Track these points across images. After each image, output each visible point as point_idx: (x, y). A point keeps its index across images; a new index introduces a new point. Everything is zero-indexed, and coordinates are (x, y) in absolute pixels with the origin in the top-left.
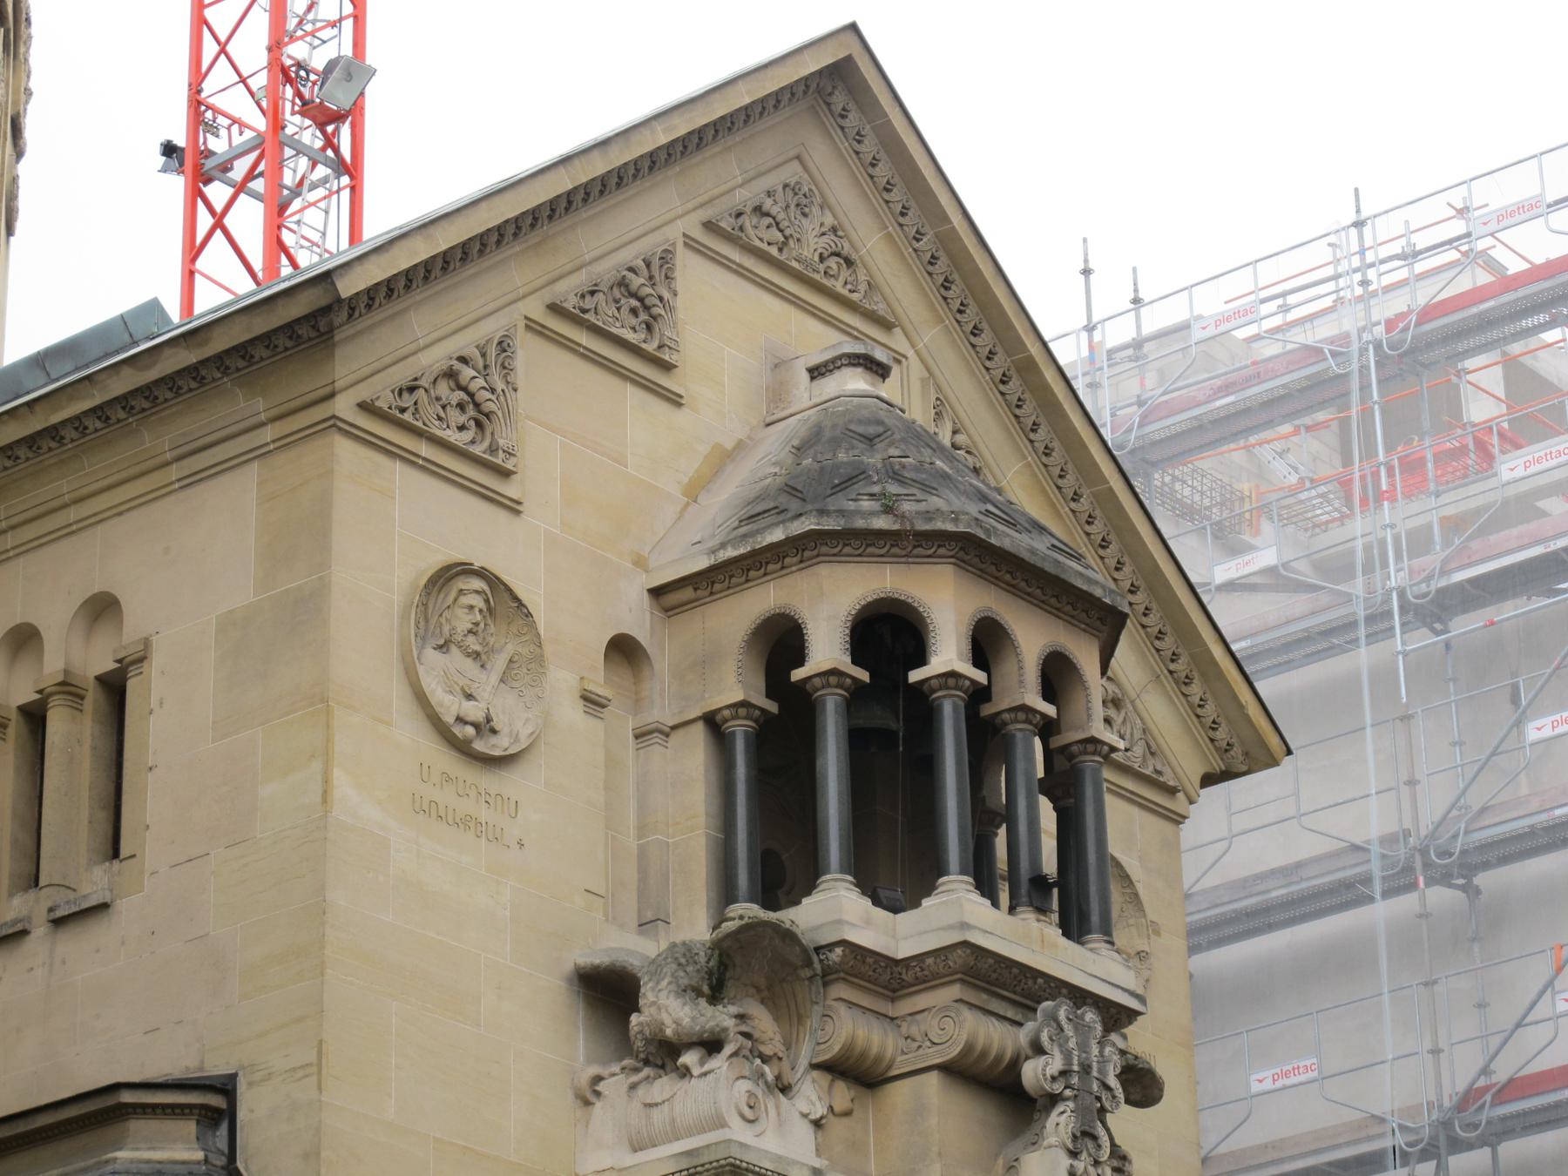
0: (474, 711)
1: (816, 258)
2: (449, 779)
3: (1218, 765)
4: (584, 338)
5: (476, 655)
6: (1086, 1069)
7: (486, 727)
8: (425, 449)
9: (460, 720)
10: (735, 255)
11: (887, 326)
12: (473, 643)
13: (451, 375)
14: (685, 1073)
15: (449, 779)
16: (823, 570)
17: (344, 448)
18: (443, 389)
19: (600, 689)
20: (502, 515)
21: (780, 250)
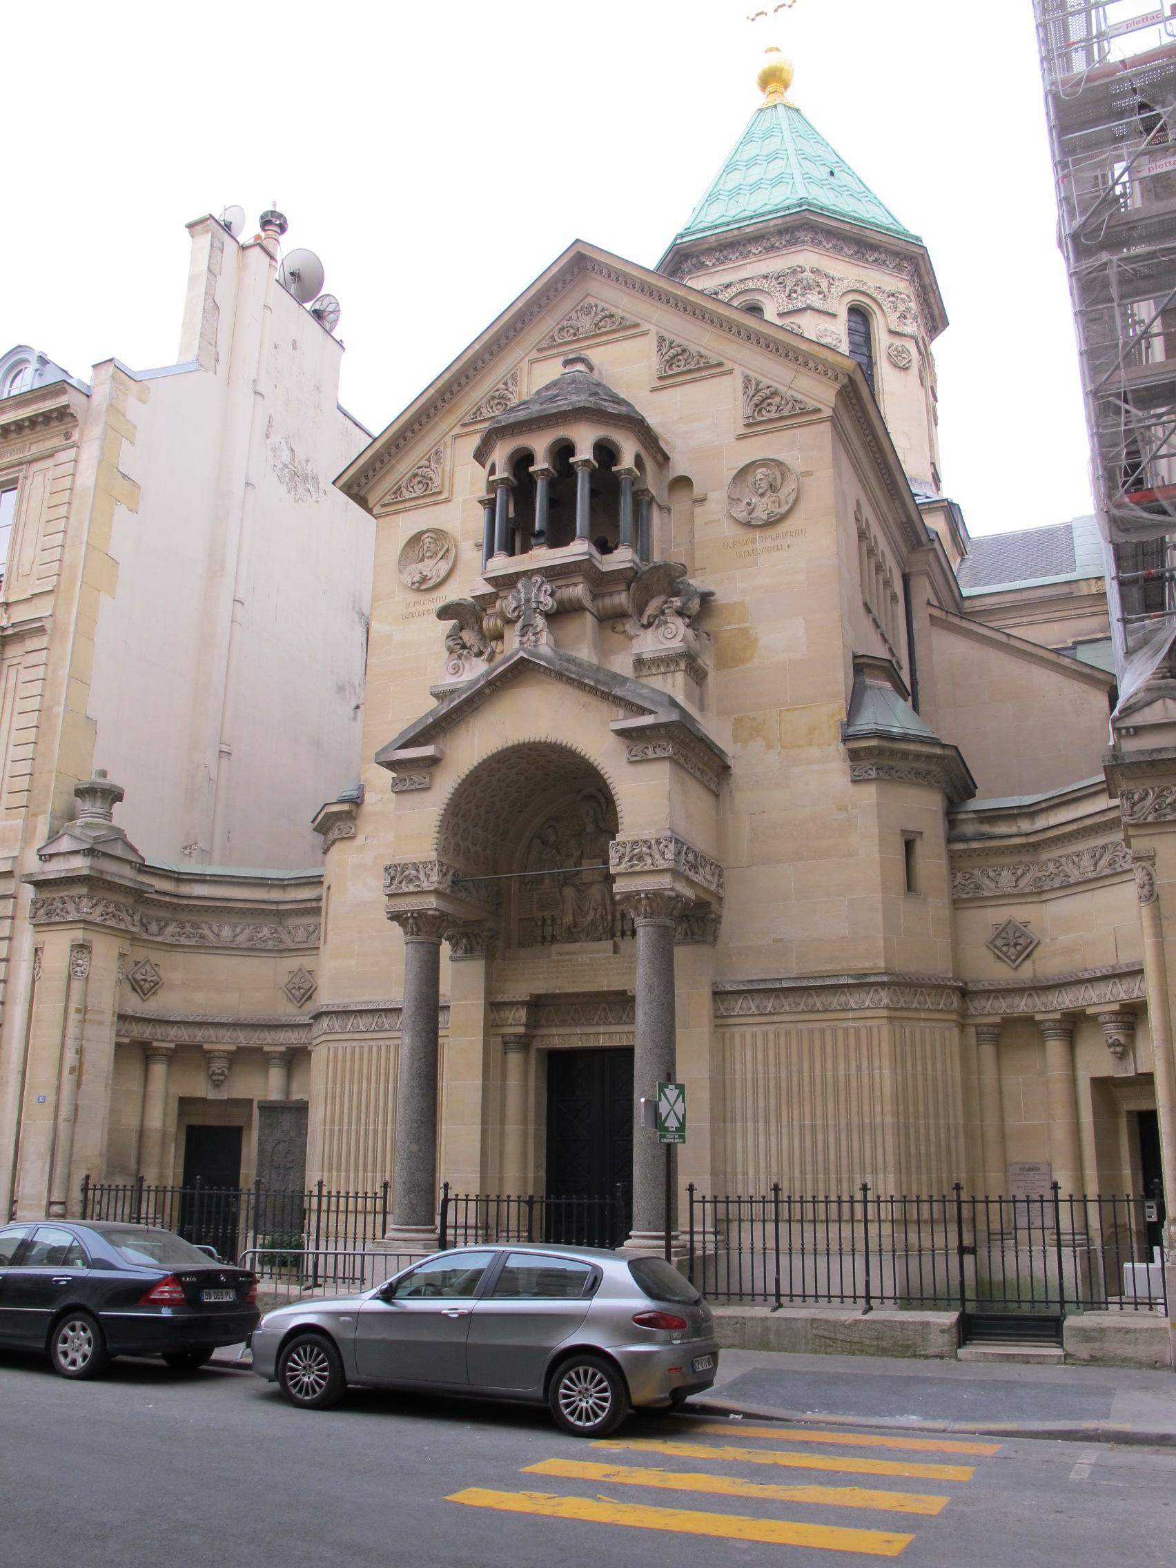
1: (593, 327)
3: (838, 386)
6: (528, 601)
7: (424, 579)
8: (407, 505)
9: (413, 583)
11: (637, 325)
13: (415, 475)
18: (415, 481)
20: (443, 506)
21: (575, 335)
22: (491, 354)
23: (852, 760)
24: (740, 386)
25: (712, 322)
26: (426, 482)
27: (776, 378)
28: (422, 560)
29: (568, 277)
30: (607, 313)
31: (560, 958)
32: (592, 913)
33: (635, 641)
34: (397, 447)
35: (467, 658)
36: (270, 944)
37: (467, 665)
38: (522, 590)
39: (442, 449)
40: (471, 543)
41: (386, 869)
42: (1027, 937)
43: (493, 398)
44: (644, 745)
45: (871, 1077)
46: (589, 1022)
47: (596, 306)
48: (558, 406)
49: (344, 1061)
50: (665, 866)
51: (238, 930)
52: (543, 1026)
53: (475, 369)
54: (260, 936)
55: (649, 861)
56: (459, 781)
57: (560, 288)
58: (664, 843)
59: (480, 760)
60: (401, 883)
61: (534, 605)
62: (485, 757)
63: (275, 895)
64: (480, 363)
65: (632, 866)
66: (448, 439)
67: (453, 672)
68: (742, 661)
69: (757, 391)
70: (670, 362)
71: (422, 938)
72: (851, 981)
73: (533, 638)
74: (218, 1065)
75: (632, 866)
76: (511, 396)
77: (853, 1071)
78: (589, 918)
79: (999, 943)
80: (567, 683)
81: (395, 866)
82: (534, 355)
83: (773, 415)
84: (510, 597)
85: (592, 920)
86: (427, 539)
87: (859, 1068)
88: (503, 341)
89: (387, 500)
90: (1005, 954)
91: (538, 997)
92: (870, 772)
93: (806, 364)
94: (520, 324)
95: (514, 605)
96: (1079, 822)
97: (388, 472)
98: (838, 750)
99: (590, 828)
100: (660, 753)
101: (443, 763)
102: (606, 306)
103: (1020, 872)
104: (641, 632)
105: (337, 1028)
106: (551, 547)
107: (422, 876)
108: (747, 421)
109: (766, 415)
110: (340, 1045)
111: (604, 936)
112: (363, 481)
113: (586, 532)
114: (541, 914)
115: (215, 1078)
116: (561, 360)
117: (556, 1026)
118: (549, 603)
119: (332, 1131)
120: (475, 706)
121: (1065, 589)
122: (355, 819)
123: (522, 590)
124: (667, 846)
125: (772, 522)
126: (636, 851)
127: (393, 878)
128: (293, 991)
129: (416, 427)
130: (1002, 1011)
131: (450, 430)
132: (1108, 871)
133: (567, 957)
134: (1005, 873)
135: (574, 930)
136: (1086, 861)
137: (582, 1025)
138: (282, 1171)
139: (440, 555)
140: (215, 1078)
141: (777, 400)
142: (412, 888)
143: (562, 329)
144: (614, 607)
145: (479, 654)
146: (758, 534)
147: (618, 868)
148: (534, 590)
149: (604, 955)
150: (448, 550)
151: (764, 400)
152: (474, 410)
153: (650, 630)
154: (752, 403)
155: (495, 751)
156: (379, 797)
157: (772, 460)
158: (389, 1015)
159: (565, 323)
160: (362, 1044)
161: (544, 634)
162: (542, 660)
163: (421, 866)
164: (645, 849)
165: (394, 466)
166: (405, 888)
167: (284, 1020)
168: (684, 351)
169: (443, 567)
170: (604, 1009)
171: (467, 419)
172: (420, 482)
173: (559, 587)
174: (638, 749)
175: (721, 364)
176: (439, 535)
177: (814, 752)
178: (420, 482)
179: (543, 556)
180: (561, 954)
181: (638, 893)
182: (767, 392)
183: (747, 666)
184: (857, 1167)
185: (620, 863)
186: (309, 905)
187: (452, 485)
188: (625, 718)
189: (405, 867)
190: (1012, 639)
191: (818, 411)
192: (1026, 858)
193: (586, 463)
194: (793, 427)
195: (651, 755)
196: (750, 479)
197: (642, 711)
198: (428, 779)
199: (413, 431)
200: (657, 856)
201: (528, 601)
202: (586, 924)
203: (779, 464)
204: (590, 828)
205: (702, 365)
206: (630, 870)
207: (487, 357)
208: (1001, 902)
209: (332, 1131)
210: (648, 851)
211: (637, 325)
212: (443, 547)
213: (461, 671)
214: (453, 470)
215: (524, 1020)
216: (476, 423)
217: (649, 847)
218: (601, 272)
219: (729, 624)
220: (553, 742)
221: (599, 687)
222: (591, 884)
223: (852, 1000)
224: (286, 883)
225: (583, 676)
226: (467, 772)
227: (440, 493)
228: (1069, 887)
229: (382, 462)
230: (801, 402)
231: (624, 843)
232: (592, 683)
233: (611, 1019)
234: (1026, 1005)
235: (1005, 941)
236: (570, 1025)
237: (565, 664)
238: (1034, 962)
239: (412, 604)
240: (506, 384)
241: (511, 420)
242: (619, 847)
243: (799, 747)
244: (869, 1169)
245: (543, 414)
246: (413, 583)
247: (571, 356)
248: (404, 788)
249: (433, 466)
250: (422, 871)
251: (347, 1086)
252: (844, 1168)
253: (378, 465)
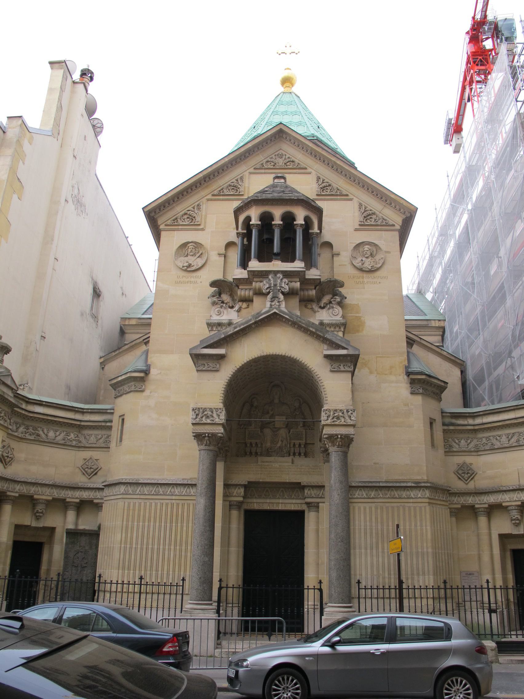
0: (186, 264)
2: (184, 276)
3: (404, 217)
4: (221, 197)
5: (193, 255)
6: (275, 285)
7: (190, 266)
8: (180, 227)
9: (183, 267)
10: (263, 171)
11: (306, 169)
12: (191, 254)
13: (186, 214)
15: (184, 276)
18: (186, 217)
20: (200, 232)
21: (274, 166)
22: (232, 164)
23: (411, 383)
24: (357, 206)
25: (346, 175)
26: (192, 218)
27: (374, 207)
28: (187, 256)
29: (273, 139)
30: (291, 160)
31: (263, 464)
32: (280, 443)
33: (317, 314)
34: (178, 198)
35: (225, 308)
36: (74, 443)
37: (225, 311)
38: (272, 279)
39: (201, 204)
40: (216, 252)
41: (193, 410)
42: (473, 470)
43: (230, 186)
44: (339, 364)
45: (422, 530)
46: (274, 497)
47: (285, 155)
48: (289, 196)
49: (134, 510)
50: (351, 423)
51: (58, 433)
52: (249, 498)
53: (223, 170)
54: (69, 438)
55: (343, 420)
56: (236, 369)
57: (268, 143)
58: (351, 412)
59: (248, 360)
60: (202, 417)
61: (278, 288)
62: (251, 359)
63: (78, 417)
64: (225, 168)
65: (333, 422)
66: (204, 200)
67: (218, 314)
68: (358, 331)
69: (365, 211)
70: (323, 189)
71: (212, 448)
72: (413, 485)
73: (277, 304)
74: (40, 508)
75: (333, 422)
76: (240, 187)
77: (413, 527)
78: (279, 445)
79: (460, 472)
80: (297, 328)
81: (199, 409)
82: (252, 170)
83: (372, 223)
84: (265, 282)
85: (280, 447)
86: (191, 246)
87: (416, 526)
88: (239, 160)
89: (169, 222)
90: (463, 477)
91: (249, 482)
92: (419, 390)
93: (391, 204)
94: (247, 154)
95: (267, 286)
96: (503, 422)
97: (171, 209)
98: (404, 378)
99: (276, 401)
100: (347, 369)
101: (226, 358)
102: (291, 157)
103: (469, 441)
104: (320, 310)
105: (131, 492)
106: (282, 262)
107: (215, 415)
108: (361, 223)
109: (369, 222)
110: (131, 501)
111: (286, 455)
112: (158, 211)
113: (301, 258)
114: (250, 441)
115: (38, 514)
116: (273, 176)
117: (256, 498)
118: (286, 288)
119: (125, 548)
120: (246, 332)
121: (425, 323)
122: (144, 381)
123: (272, 279)
124: (352, 414)
125: (372, 271)
126: (336, 415)
127: (197, 415)
128: (86, 469)
129: (190, 190)
130: (461, 503)
131: (206, 196)
132: (516, 444)
133: (267, 464)
134: (462, 441)
135: (270, 450)
136: (504, 439)
137: (270, 498)
138: (79, 568)
139: (198, 255)
140: (38, 514)
141: (374, 217)
142: (209, 421)
143: (268, 162)
144: (309, 295)
145: (232, 307)
146: (365, 275)
147: (327, 422)
148: (279, 281)
149: (287, 464)
150: (202, 254)
151: (368, 215)
152: (219, 189)
153: (325, 310)
154: (363, 216)
155: (256, 356)
156: (159, 372)
157: (372, 243)
158: (163, 487)
159: (269, 160)
160: (146, 501)
161: (284, 303)
162: (286, 315)
163: (214, 410)
164: (341, 414)
165: (174, 207)
166: (204, 420)
167: (80, 485)
168: (330, 185)
169: (200, 262)
170: (282, 491)
171: (216, 192)
172: (188, 218)
173: (291, 282)
174: (336, 365)
175: (347, 195)
176: (198, 245)
177: (393, 378)
178: (188, 218)
179: (277, 265)
180: (263, 462)
181: (337, 435)
182: (371, 212)
183: (360, 334)
184: (415, 572)
185: (327, 419)
186: (100, 424)
187: (205, 223)
188: (328, 350)
189: (205, 410)
190: (422, 340)
191: (393, 225)
192: (471, 436)
193: (302, 225)
194: (381, 230)
195: (342, 368)
196: (361, 249)
197: (338, 347)
198: (218, 366)
199: (187, 192)
200: (347, 418)
201: (275, 285)
202: (276, 448)
203: (376, 245)
204: (276, 401)
205: (338, 193)
206: (332, 423)
207: (230, 165)
208: (460, 454)
209: (125, 548)
210: (342, 415)
211: (306, 169)
212: (199, 252)
213: (222, 314)
214: (206, 216)
215: (242, 494)
216: (220, 195)
217: (343, 413)
218: (290, 140)
219: (351, 313)
220: (289, 356)
221: (318, 332)
222: (279, 429)
223: (412, 494)
224: (85, 411)
225: (309, 327)
226: (240, 365)
227: (199, 225)
228: (493, 450)
229: (169, 204)
230: (386, 220)
231: (330, 410)
232: (314, 330)
233: (286, 496)
234: (472, 501)
235: (463, 472)
236: (264, 498)
237: (299, 319)
238: (474, 481)
239: (181, 277)
240: (237, 180)
241: (264, 197)
242: (327, 412)
243: (386, 374)
244: (421, 573)
245: (281, 198)
246: (183, 267)
247: (279, 175)
248: (204, 369)
249: (196, 212)
250: (214, 412)
251: (136, 523)
252: (409, 573)
253: (167, 205)
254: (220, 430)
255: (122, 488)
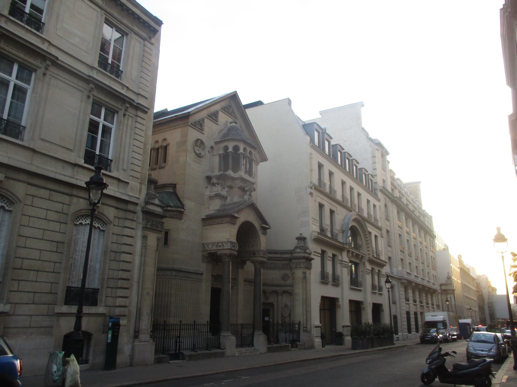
0: (199, 152)
7: (200, 154)
8: (196, 128)
9: (198, 153)
10: (224, 111)
14: (216, 186)
16: (231, 142)
17: (189, 127)
19: (210, 151)
176: (202, 143)
254: (236, 253)
255: (174, 273)
